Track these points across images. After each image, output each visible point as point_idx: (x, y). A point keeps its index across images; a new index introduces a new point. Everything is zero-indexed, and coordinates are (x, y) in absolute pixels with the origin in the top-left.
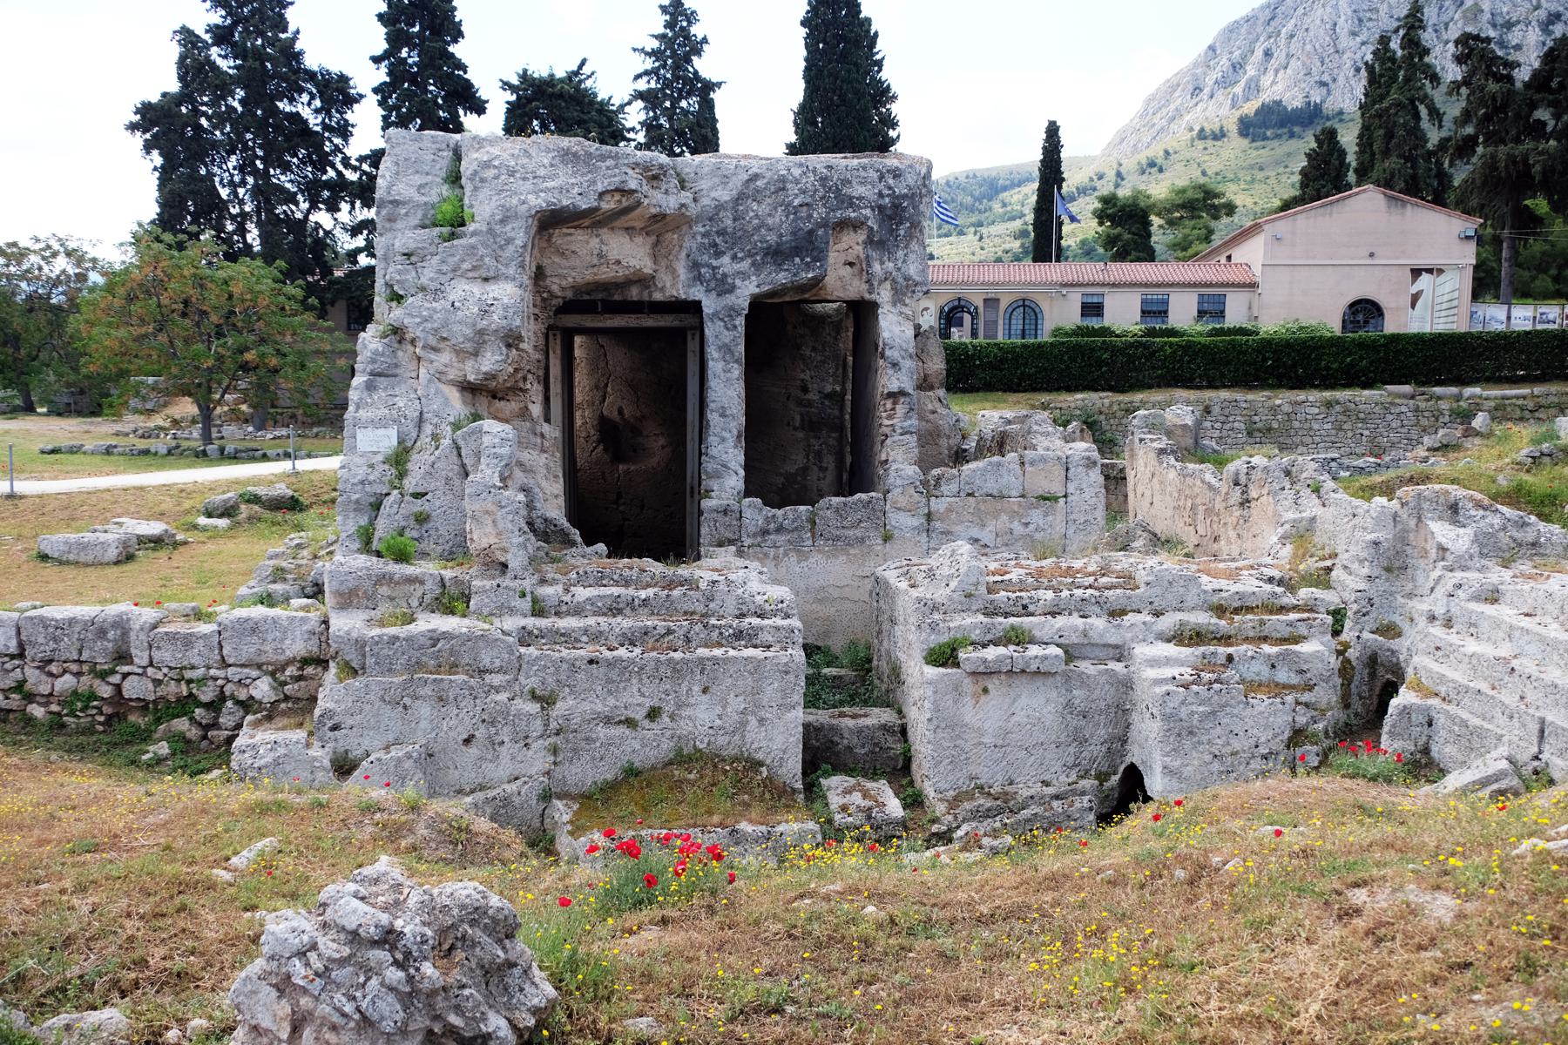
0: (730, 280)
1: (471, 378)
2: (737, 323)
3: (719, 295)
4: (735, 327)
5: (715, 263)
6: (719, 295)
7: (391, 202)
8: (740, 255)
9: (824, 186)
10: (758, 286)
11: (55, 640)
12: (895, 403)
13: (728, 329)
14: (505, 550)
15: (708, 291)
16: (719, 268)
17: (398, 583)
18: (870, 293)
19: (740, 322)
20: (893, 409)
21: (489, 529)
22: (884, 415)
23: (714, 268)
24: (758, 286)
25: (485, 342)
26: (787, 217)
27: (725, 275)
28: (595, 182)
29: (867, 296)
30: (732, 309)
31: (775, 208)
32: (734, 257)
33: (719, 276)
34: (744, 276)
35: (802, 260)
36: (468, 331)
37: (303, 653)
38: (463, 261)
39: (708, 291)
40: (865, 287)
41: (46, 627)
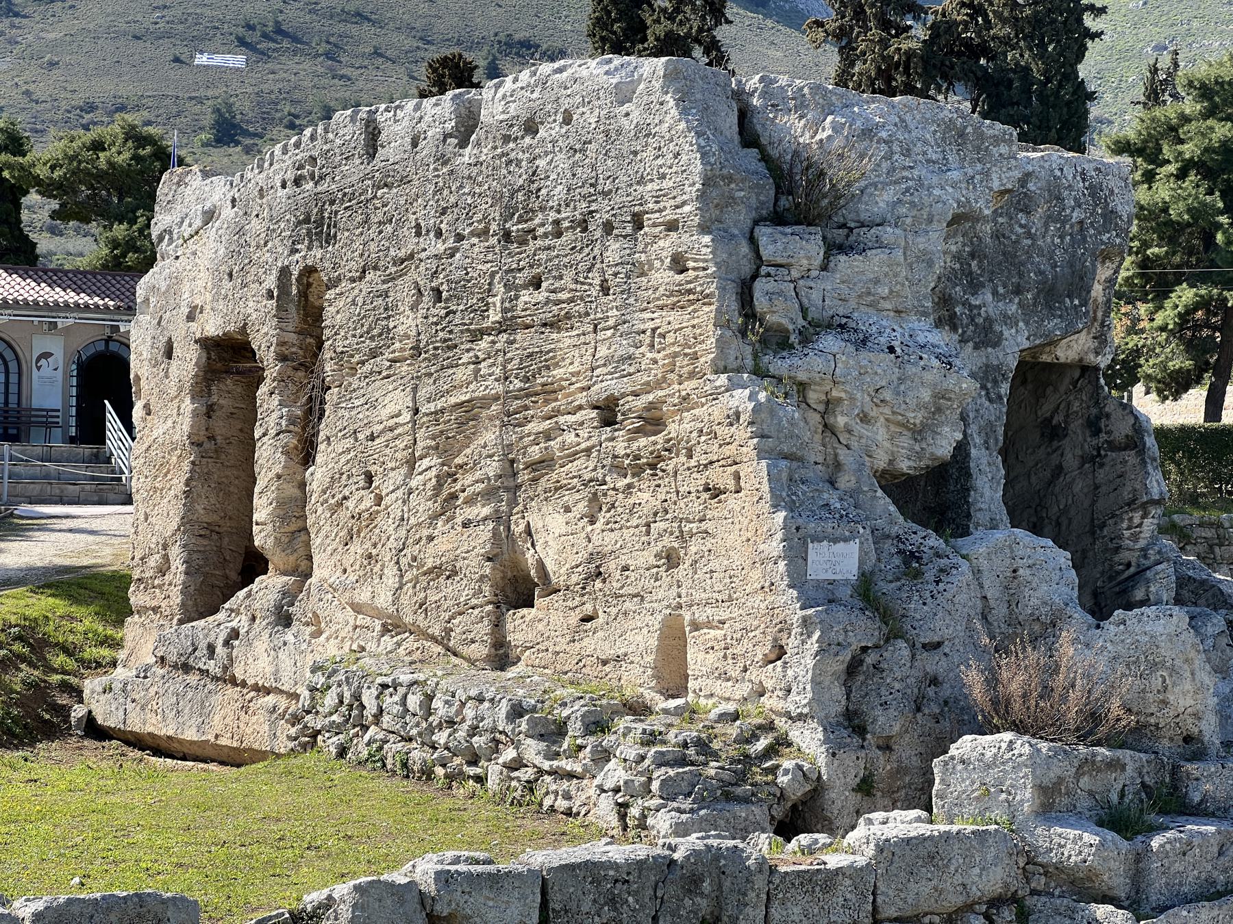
0: (997, 328)
1: (904, 466)
2: (1003, 391)
3: (976, 347)
4: (1000, 397)
5: (975, 302)
6: (976, 347)
7: (723, 178)
8: (1001, 290)
9: (1093, 195)
10: (1028, 339)
11: (613, 901)
12: (1143, 517)
13: (990, 401)
14: (1197, 716)
15: (963, 341)
16: (979, 307)
17: (1099, 770)
18: (1097, 354)
19: (1005, 388)
20: (1140, 525)
21: (1188, 686)
22: (1127, 533)
23: (971, 307)
24: (1028, 339)
25: (939, 410)
26: (1062, 237)
27: (988, 319)
28: (987, 174)
29: (1091, 357)
30: (998, 368)
31: (1046, 225)
32: (995, 293)
33: (980, 320)
34: (1008, 320)
35: (1072, 303)
36: (926, 395)
37: (998, 889)
38: (877, 281)
39: (963, 341)
40: (1092, 344)
41: (596, 881)
